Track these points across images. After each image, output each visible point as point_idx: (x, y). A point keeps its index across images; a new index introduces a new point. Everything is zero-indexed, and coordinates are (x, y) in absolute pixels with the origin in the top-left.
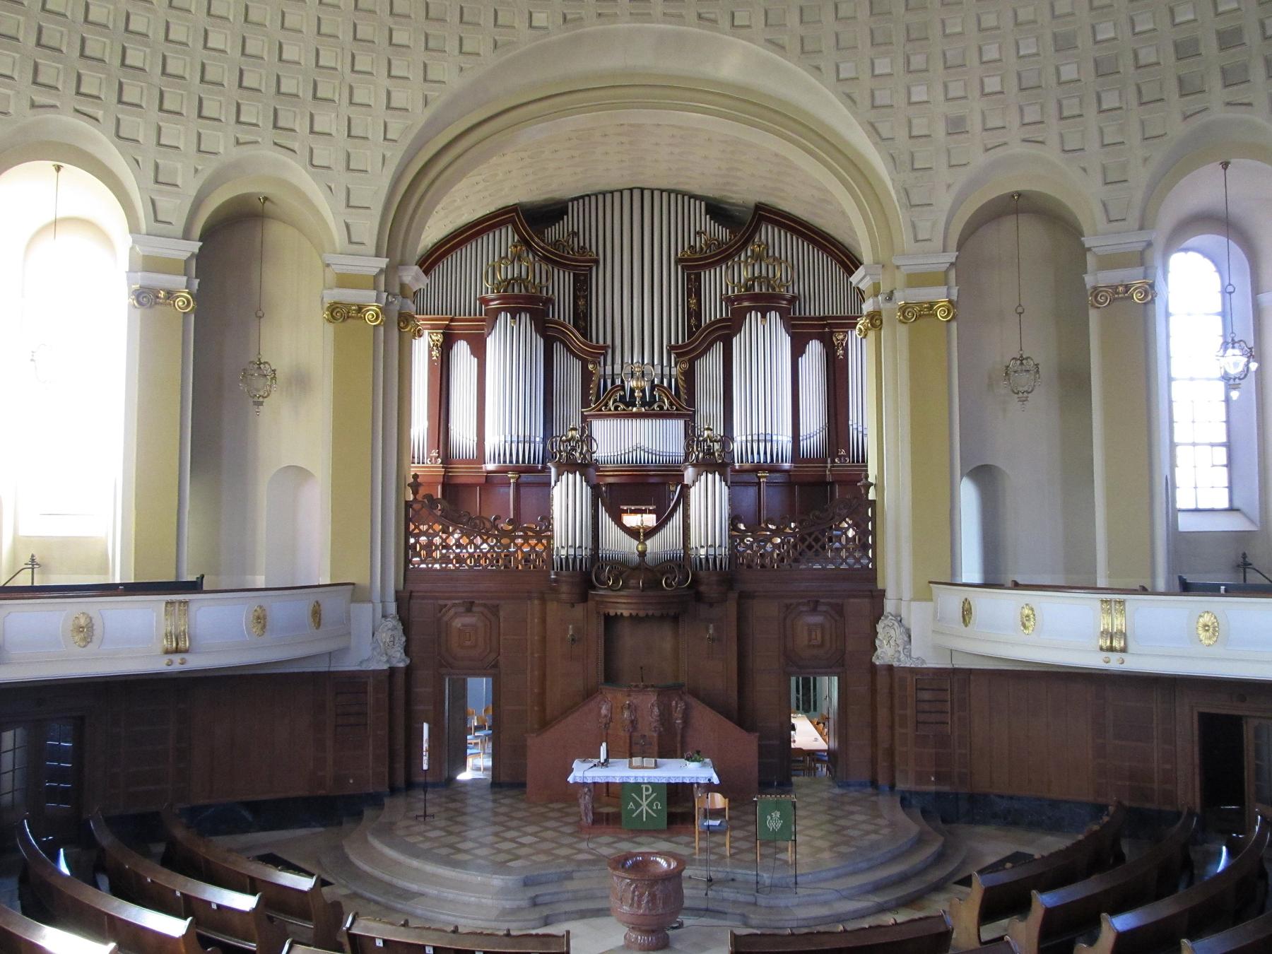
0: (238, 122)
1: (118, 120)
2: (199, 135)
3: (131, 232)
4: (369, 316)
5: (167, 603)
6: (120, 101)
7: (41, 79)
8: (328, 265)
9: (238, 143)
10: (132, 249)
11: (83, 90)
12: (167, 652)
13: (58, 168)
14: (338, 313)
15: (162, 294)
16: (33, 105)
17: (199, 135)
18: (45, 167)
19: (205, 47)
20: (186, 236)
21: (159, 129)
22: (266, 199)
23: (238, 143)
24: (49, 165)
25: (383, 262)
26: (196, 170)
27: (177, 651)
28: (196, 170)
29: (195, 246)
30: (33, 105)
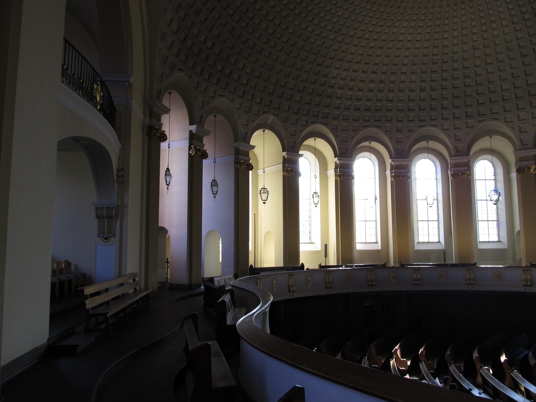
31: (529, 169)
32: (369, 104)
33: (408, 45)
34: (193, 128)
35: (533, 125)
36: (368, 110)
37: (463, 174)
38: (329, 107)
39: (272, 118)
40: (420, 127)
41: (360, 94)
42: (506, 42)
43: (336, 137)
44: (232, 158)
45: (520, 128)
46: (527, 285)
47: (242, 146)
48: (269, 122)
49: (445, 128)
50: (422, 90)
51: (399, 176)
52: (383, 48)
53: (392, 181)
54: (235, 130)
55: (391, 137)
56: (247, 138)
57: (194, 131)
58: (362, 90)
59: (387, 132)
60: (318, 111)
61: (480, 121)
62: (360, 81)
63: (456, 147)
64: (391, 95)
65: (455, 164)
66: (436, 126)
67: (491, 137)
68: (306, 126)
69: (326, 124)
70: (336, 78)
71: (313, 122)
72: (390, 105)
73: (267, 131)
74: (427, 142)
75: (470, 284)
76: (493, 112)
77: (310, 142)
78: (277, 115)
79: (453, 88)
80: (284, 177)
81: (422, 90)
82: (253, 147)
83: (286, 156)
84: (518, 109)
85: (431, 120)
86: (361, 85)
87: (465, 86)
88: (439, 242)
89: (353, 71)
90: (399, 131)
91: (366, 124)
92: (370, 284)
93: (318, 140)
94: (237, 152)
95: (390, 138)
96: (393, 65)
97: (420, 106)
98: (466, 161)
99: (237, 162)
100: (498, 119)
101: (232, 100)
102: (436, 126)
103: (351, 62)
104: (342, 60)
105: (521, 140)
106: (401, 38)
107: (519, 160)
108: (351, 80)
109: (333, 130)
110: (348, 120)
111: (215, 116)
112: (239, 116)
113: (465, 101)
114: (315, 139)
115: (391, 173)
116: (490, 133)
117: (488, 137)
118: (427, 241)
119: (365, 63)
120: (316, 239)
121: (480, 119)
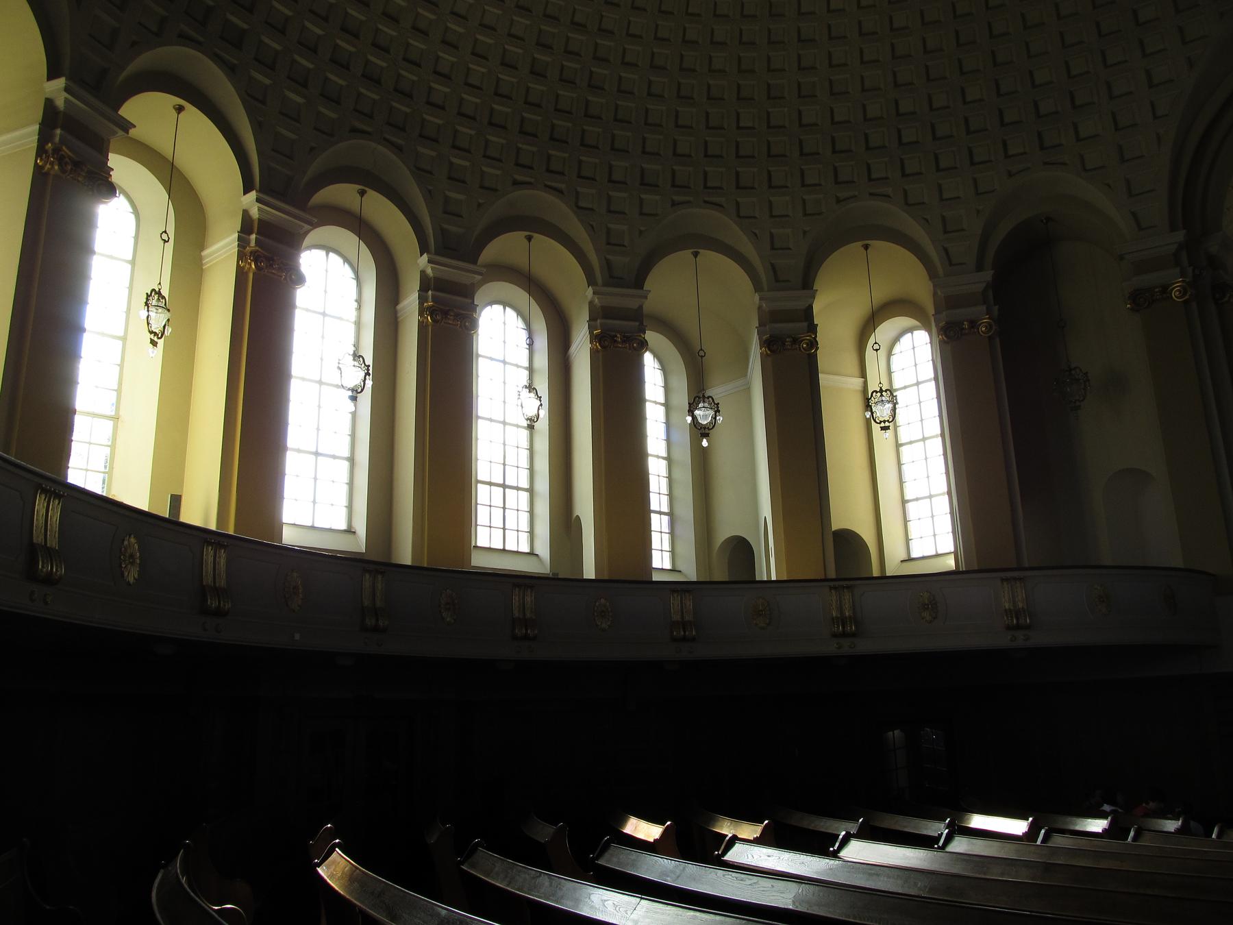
0: (1007, 156)
1: (905, 192)
2: (975, 180)
3: (931, 278)
4: (1175, 294)
5: (1003, 580)
6: (904, 175)
8: (1121, 258)
10: (935, 294)
11: (874, 176)
12: (1009, 628)
13: (866, 247)
14: (1140, 300)
15: (966, 325)
16: (838, 201)
17: (975, 180)
19: (965, 103)
20: (980, 267)
21: (940, 186)
23: (1010, 174)
24: (857, 246)
25: (1180, 236)
26: (978, 211)
27: (1018, 627)
28: (978, 211)
29: (988, 275)
30: (838, 201)
31: (795, 341)
36: (373, 79)
43: (258, 127)
46: (844, 635)
49: (582, 204)
50: (537, 73)
51: (445, 314)
53: (422, 327)
55: (430, 191)
59: (422, 173)
61: (674, 204)
63: (609, 265)
65: (603, 308)
66: (560, 191)
67: (696, 254)
69: (231, 70)
71: (184, 39)
75: (684, 639)
79: (619, 91)
81: (537, 73)
92: (370, 622)
93: (195, 118)
95: (429, 195)
97: (523, 120)
100: (721, 206)
102: (560, 191)
107: (769, 318)
109: (254, 100)
115: (422, 299)
116: (699, 241)
117: (687, 254)
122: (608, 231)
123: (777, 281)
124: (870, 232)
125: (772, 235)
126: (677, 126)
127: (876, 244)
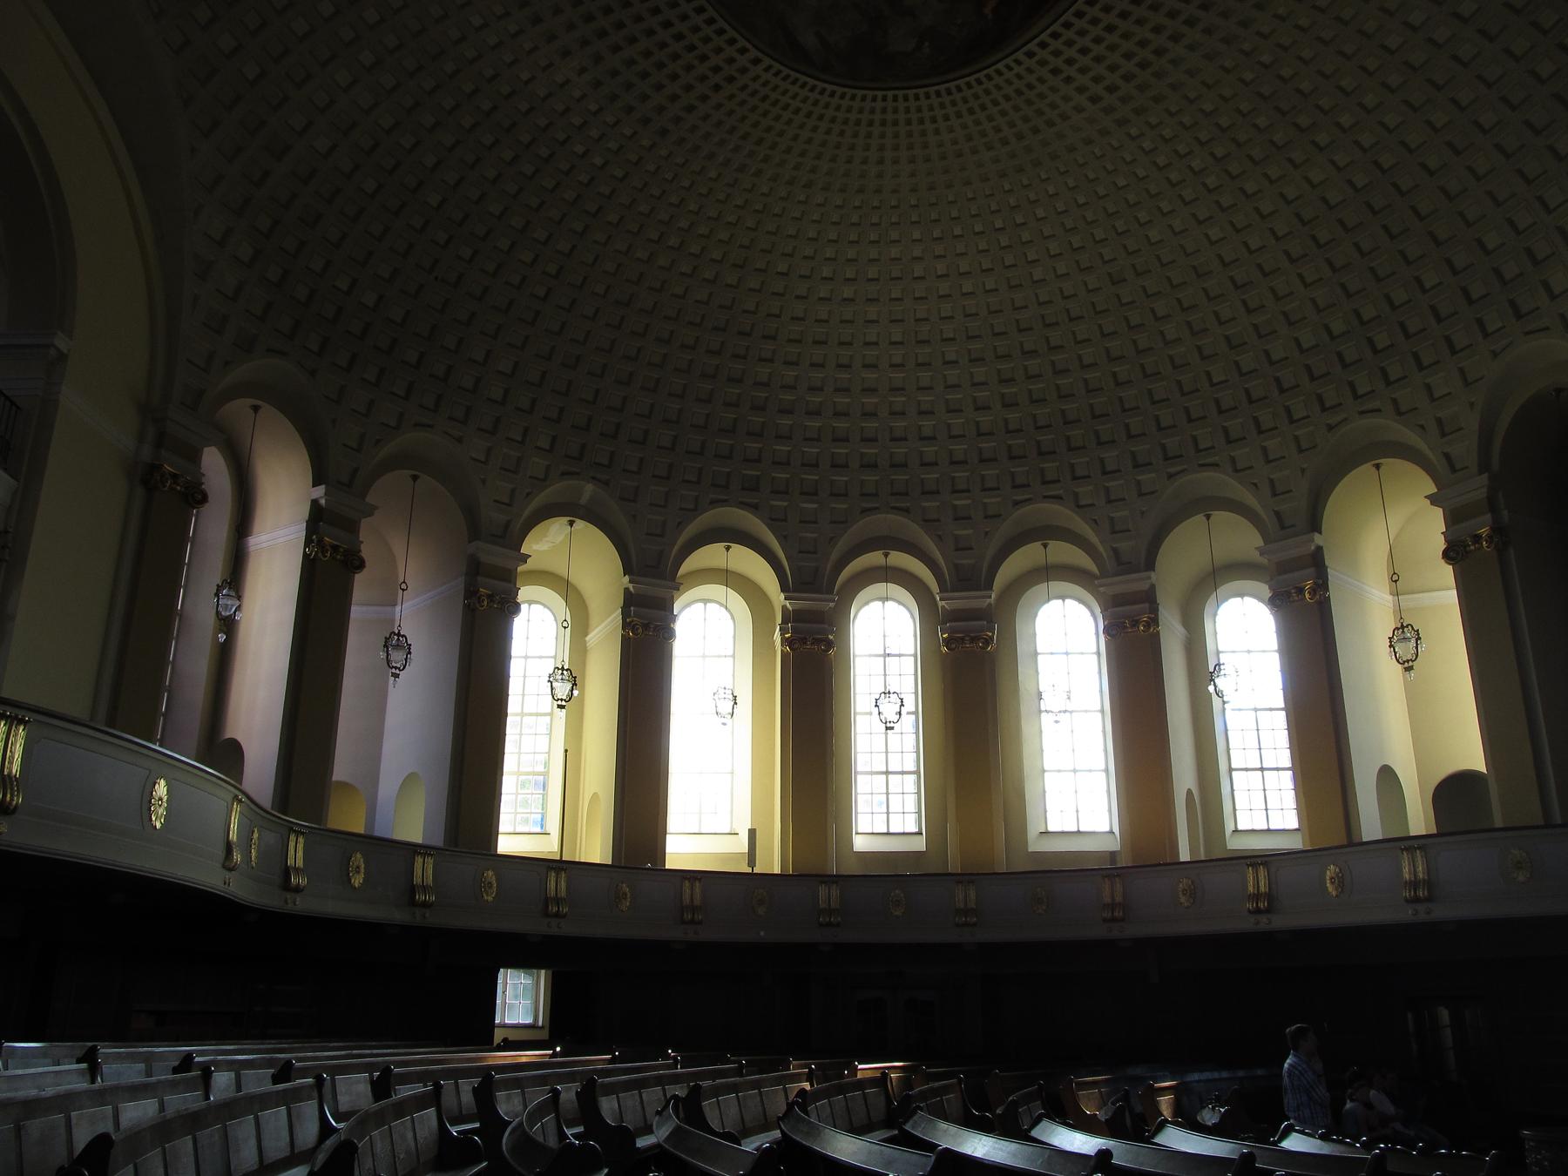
2: (1461, 371)
7: (1328, 404)
9: (1495, 355)
13: (1378, 467)
16: (1330, 428)
18: (1366, 469)
22: (1559, 391)
23: (1495, 355)
31: (1301, 591)
32: (871, 451)
33: (944, 287)
34: (319, 492)
35: (1303, 470)
37: (1135, 623)
38: (758, 461)
39: (589, 489)
40: (1016, 503)
41: (841, 424)
42: (1188, 255)
43: (783, 539)
44: (460, 584)
45: (1272, 481)
47: (491, 555)
48: (583, 501)
49: (1083, 502)
50: (1009, 404)
52: (877, 300)
54: (471, 514)
56: (511, 537)
57: (323, 502)
58: (846, 414)
59: (928, 523)
60: (729, 474)
61: (1170, 476)
62: (837, 390)
64: (927, 424)
67: (1208, 517)
68: (696, 511)
69: (754, 508)
70: (767, 385)
71: (715, 503)
72: (930, 450)
73: (580, 524)
74: (1045, 546)
76: (1202, 447)
77: (711, 555)
78: (607, 483)
80: (626, 644)
81: (1009, 404)
82: (525, 558)
83: (631, 587)
84: (1260, 432)
85: (1044, 483)
86: (842, 400)
87: (1118, 384)
88: (1111, 832)
89: (812, 365)
90: (961, 518)
91: (865, 505)
94: (475, 569)
95: (939, 539)
96: (919, 342)
98: (1145, 586)
99: (471, 593)
101: (460, 440)
102: (1058, 498)
103: (799, 341)
104: (774, 338)
105: (1278, 514)
106: (918, 270)
108: (811, 389)
109: (774, 522)
110: (816, 494)
111: (415, 478)
112: (484, 481)
113: (1127, 426)
114: (728, 548)
116: (1207, 504)
117: (1200, 518)
118: (1074, 829)
119: (841, 344)
120: (718, 807)
121: (1172, 470)
122: (1112, 519)
123: (1283, 527)
124: (1376, 451)
125: (1272, 481)
126: (1154, 403)
127: (1387, 463)
